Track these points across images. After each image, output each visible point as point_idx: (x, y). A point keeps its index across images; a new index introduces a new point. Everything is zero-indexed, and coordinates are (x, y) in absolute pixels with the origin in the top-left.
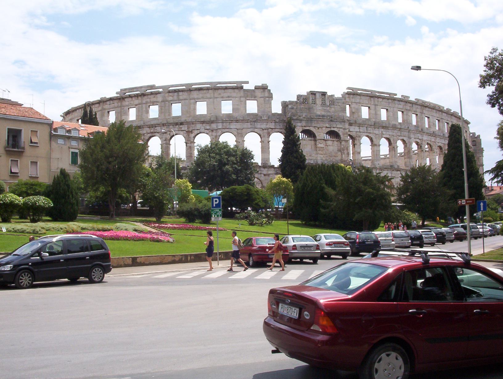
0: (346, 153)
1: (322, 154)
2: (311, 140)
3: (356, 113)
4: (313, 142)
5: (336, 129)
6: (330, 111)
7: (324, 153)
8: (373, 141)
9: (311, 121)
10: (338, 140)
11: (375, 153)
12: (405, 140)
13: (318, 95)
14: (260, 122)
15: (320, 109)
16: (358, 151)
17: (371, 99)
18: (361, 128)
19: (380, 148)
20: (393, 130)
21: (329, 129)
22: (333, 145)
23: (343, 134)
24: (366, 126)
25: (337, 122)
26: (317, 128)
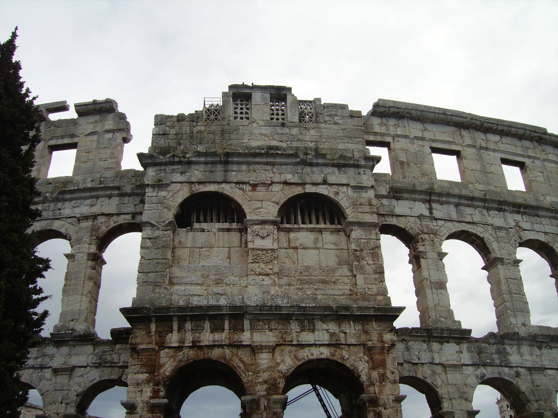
0: (369, 269)
1: (268, 275)
2: (229, 230)
3: (412, 165)
4: (235, 237)
5: (323, 190)
6: (300, 137)
7: (276, 270)
8: (490, 250)
9: (226, 163)
10: (339, 226)
11: (504, 288)
13: (257, 97)
14: (71, 200)
15: (263, 131)
16: (435, 277)
17: (461, 135)
18: (434, 205)
19: (519, 271)
21: (298, 190)
22: (319, 245)
23: (355, 204)
26: (248, 188)
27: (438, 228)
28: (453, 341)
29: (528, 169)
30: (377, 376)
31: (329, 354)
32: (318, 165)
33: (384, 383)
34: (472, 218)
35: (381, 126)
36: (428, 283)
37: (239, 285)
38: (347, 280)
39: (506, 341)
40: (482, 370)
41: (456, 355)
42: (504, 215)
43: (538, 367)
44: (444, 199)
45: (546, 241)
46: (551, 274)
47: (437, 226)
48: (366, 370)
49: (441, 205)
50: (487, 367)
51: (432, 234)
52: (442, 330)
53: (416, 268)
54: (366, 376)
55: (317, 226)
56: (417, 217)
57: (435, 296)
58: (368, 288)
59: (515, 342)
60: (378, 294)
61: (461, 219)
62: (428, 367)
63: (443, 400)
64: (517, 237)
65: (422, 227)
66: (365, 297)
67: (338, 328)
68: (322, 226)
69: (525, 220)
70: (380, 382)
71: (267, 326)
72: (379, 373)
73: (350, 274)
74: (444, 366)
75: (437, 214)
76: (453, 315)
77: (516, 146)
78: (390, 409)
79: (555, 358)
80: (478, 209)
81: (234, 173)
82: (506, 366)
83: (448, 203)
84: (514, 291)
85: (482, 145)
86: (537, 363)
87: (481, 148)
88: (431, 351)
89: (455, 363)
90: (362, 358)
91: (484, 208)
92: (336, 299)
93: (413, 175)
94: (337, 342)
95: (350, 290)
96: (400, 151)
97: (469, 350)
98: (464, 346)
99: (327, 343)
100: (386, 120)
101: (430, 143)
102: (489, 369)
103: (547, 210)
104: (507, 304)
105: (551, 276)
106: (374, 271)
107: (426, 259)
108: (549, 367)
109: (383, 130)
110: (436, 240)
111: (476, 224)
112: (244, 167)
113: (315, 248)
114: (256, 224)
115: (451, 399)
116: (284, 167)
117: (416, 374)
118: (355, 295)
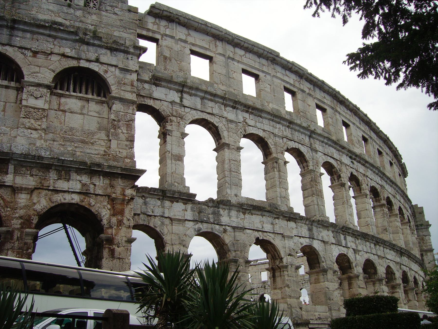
0: (123, 137)
1: (36, 130)
2: (7, 87)
3: (173, 61)
4: (12, 94)
5: (94, 67)
6: (83, 19)
7: (44, 126)
8: (222, 136)
9: (12, 28)
10: (104, 99)
11: (226, 166)
12: (302, 151)
15: (51, 8)
16: (175, 151)
17: (215, 44)
18: (185, 96)
19: (240, 156)
20: (273, 120)
21: (73, 63)
22: (85, 111)
24: (202, 95)
25: (99, 46)
26: (29, 54)
27: (185, 113)
28: (182, 201)
29: (260, 81)
30: (116, 221)
31: (78, 200)
32: (94, 45)
33: (120, 227)
34: (212, 110)
35: (154, 25)
36: (170, 155)
37: (9, 135)
38: (103, 143)
39: (221, 206)
40: (199, 225)
41: (182, 212)
42: (236, 112)
43: (240, 227)
44: (193, 92)
45: (263, 136)
46: (263, 161)
47: (184, 112)
48: (108, 216)
49: (190, 96)
50: (203, 223)
51: (180, 117)
52: (174, 192)
53: (163, 141)
54: (107, 220)
55: (86, 96)
56: (170, 102)
57: (173, 165)
58: (120, 152)
59: (227, 207)
60: (126, 157)
61: (204, 110)
62: (159, 219)
63: (167, 245)
64: (243, 130)
65: (172, 110)
66: (115, 159)
67: (89, 181)
68: (90, 96)
69: (251, 118)
70: (117, 226)
71: (29, 172)
72: (117, 219)
73: (107, 138)
74: (171, 219)
75: (185, 102)
76: (185, 182)
77: (255, 62)
78: (122, 248)
79: (253, 222)
80: (218, 104)
81: (18, 39)
82: (217, 224)
83: (196, 95)
84: (234, 170)
85: (230, 56)
86: (240, 224)
87: (229, 58)
88: (163, 207)
89: (180, 218)
90: (105, 206)
91: (222, 104)
92: (91, 157)
93: (172, 69)
94: (87, 192)
95: (105, 151)
96: (165, 48)
97: (192, 209)
98: (189, 206)
99: (78, 191)
100: (159, 21)
101: (190, 46)
102: (205, 225)
103: (269, 113)
104: (227, 179)
105: (262, 163)
106: (127, 138)
107: (172, 136)
108: (248, 228)
109: (155, 28)
110: (181, 122)
111: (214, 115)
112: (28, 35)
113: (81, 114)
114: (32, 86)
115: (172, 245)
116: (64, 42)
117: (149, 223)
118: (107, 156)
